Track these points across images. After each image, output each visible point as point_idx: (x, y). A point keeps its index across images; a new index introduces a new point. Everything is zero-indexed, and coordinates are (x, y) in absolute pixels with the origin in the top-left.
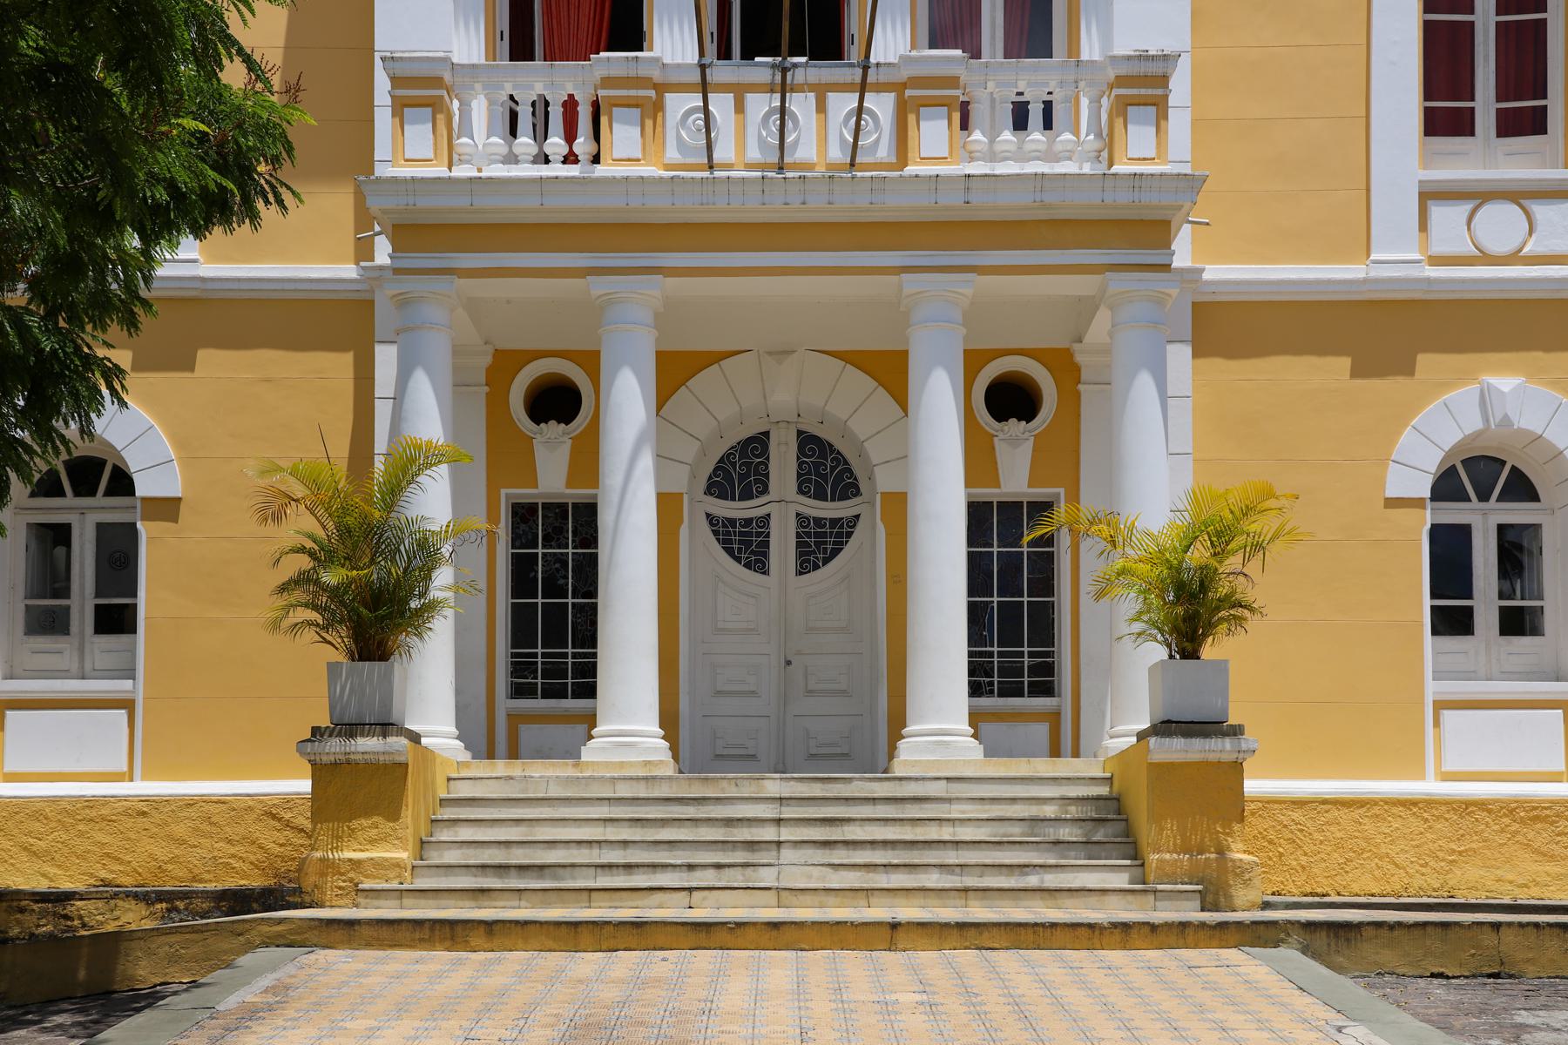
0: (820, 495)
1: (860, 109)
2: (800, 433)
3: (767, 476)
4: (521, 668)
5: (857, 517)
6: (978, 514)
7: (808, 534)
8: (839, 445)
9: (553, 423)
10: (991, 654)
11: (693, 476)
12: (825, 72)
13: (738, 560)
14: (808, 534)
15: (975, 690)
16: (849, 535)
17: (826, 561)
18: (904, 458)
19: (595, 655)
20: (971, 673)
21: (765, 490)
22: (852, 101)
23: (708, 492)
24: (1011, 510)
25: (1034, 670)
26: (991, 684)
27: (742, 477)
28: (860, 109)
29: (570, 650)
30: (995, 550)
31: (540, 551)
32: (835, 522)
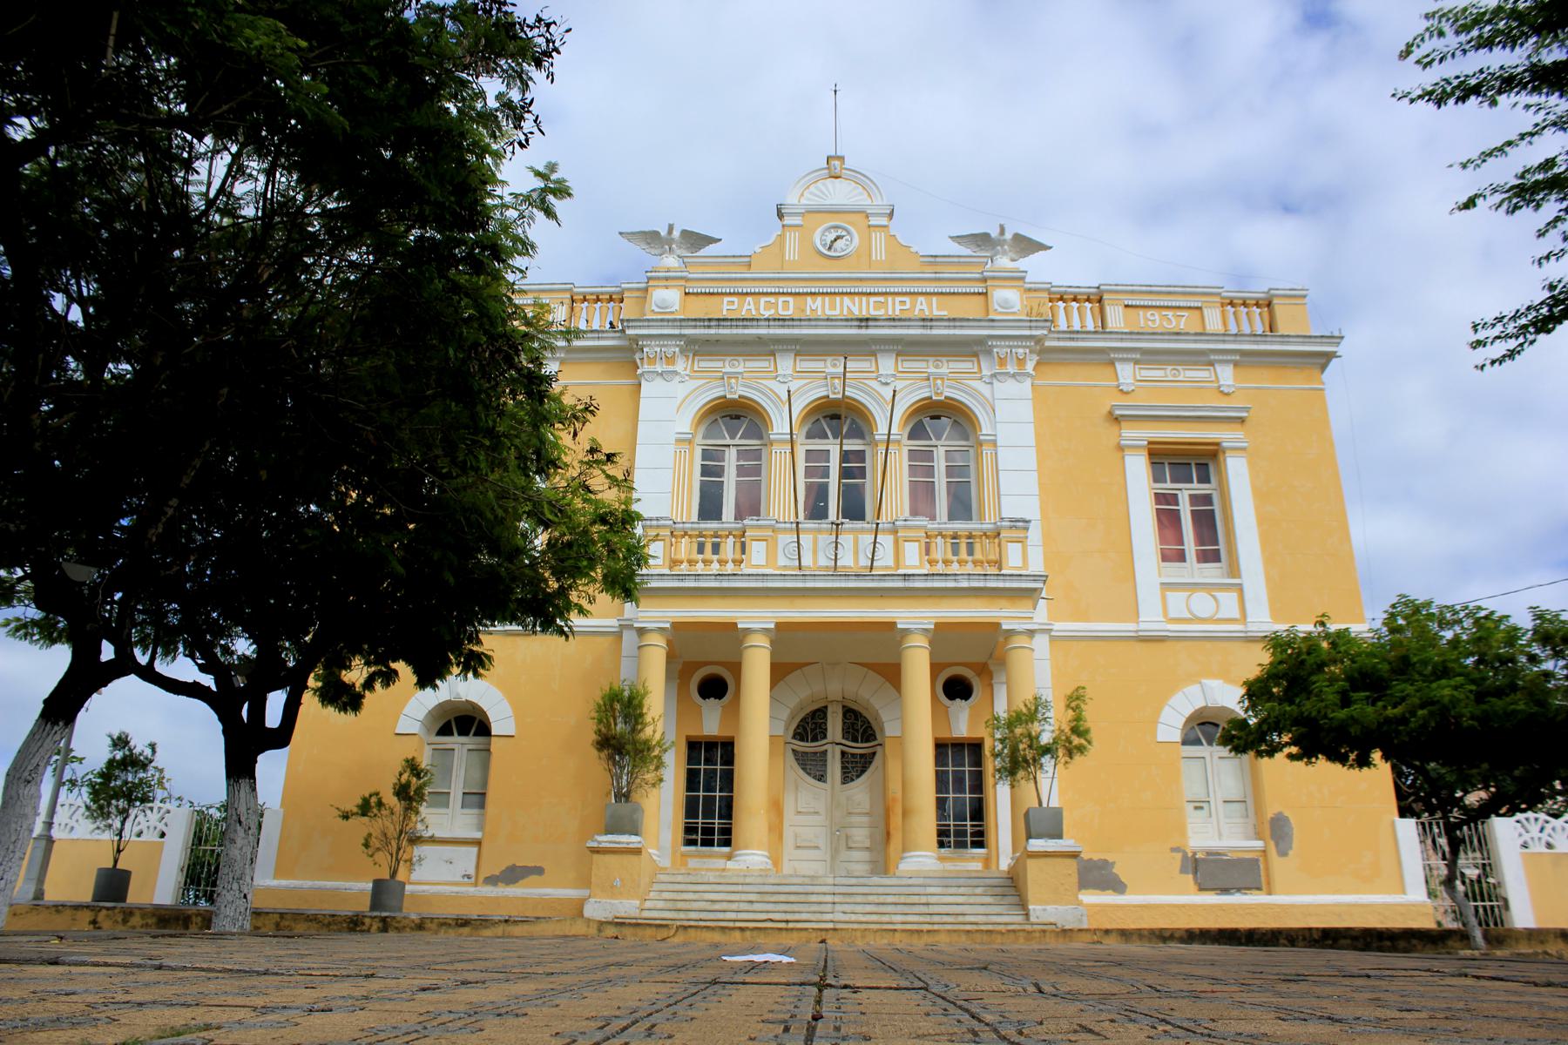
0: (855, 740)
1: (875, 542)
2: (844, 707)
3: (826, 729)
4: (689, 830)
5: (874, 753)
6: (941, 747)
7: (848, 762)
8: (865, 713)
9: (712, 699)
10: (949, 825)
11: (787, 729)
12: (858, 525)
13: (809, 774)
14: (848, 762)
15: (941, 845)
16: (870, 763)
17: (858, 776)
18: (902, 719)
19: (731, 824)
20: (939, 835)
21: (825, 737)
22: (871, 538)
23: (794, 737)
24: (959, 746)
25: (973, 835)
26: (950, 842)
27: (812, 730)
28: (875, 542)
29: (717, 821)
30: (951, 769)
31: (702, 767)
32: (862, 756)
